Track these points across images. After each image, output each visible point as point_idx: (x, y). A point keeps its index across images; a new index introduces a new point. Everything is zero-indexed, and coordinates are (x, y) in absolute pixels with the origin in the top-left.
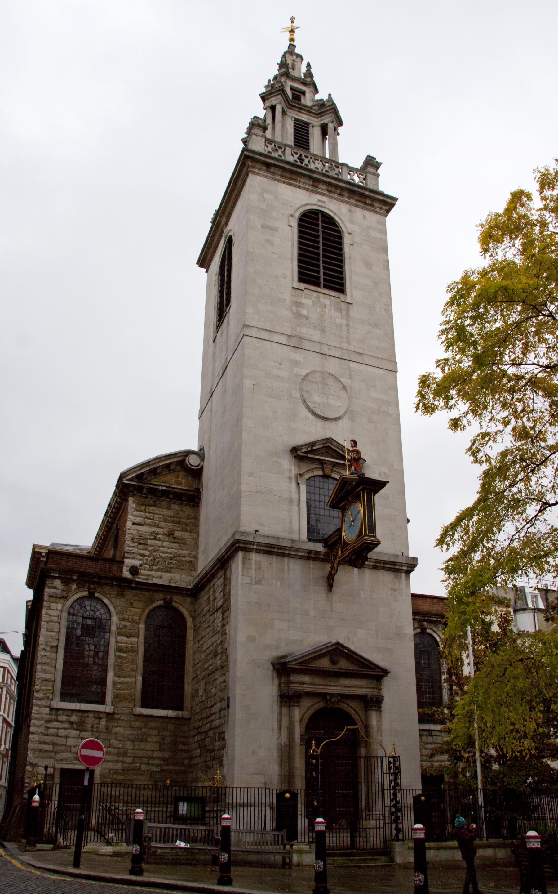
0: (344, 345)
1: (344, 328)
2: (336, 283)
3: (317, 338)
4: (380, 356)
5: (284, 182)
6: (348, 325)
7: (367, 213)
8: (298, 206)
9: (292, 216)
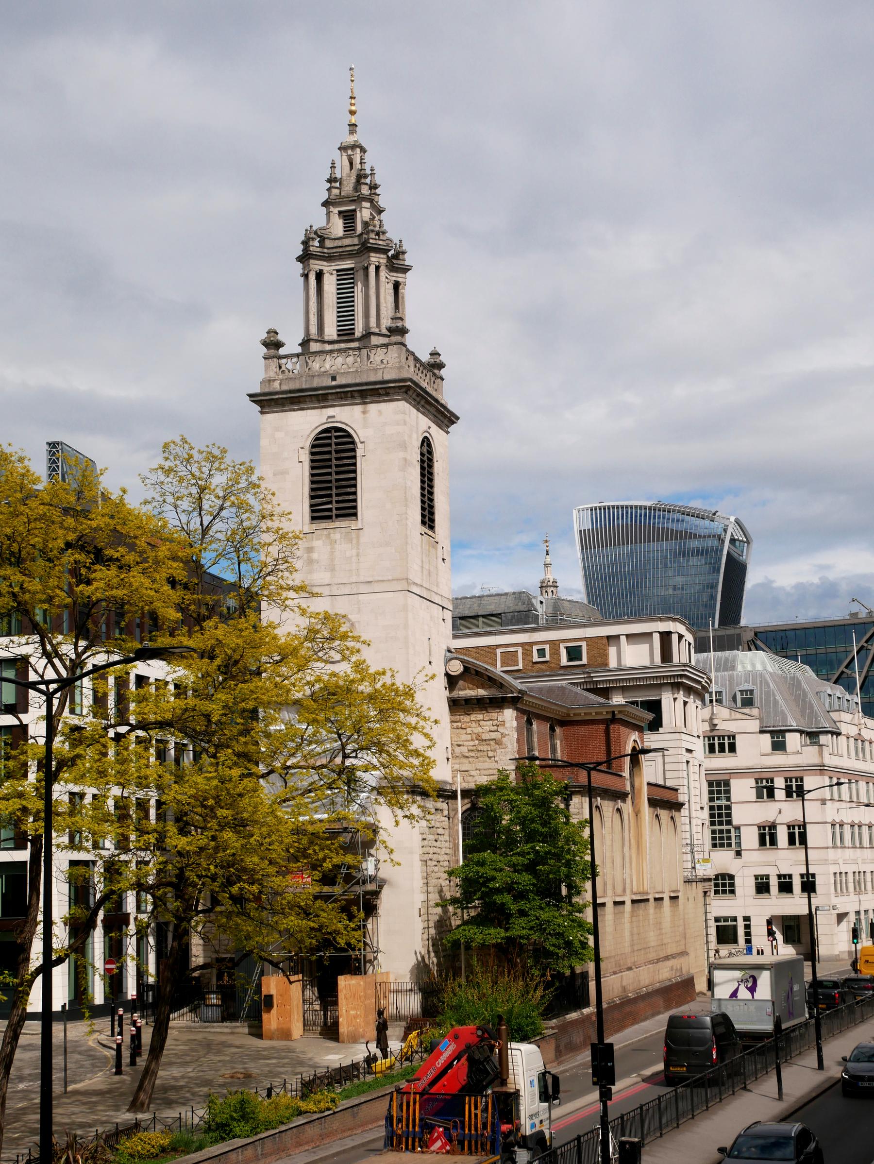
0: (354, 579)
1: (354, 559)
2: (349, 511)
3: (327, 582)
4: (390, 578)
5: (294, 410)
6: (358, 555)
7: (382, 406)
8: (308, 433)
9: (302, 448)
